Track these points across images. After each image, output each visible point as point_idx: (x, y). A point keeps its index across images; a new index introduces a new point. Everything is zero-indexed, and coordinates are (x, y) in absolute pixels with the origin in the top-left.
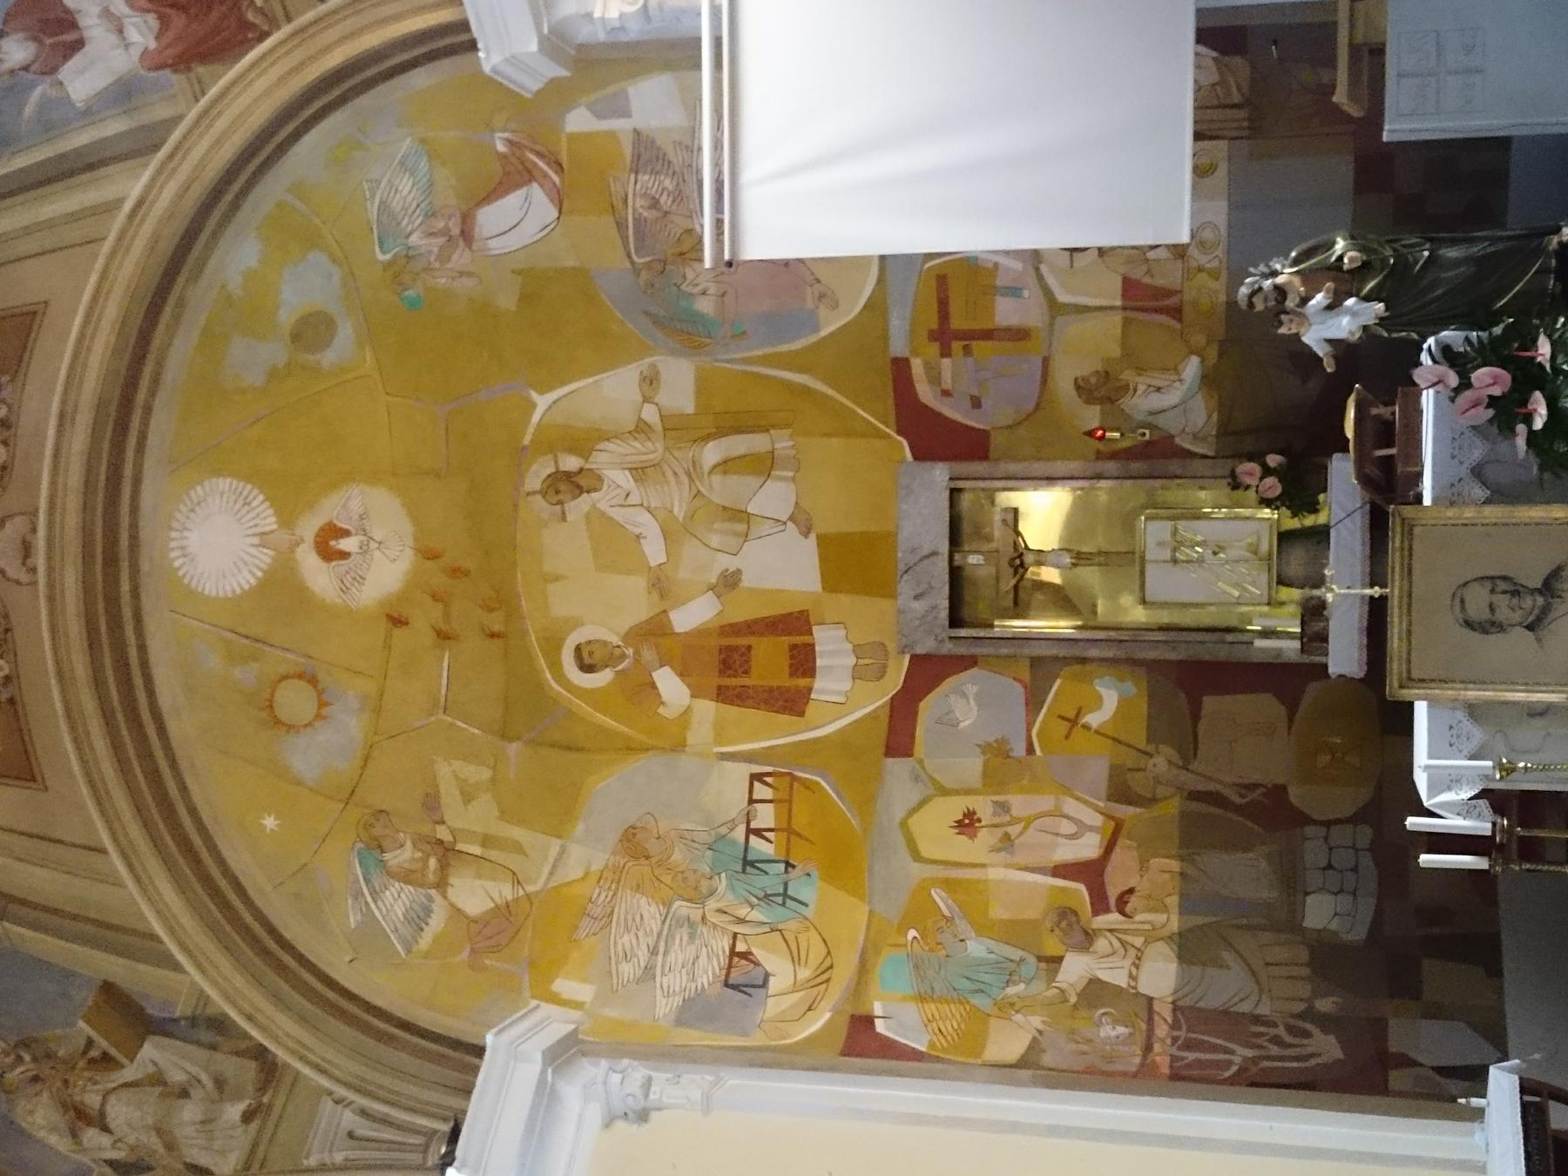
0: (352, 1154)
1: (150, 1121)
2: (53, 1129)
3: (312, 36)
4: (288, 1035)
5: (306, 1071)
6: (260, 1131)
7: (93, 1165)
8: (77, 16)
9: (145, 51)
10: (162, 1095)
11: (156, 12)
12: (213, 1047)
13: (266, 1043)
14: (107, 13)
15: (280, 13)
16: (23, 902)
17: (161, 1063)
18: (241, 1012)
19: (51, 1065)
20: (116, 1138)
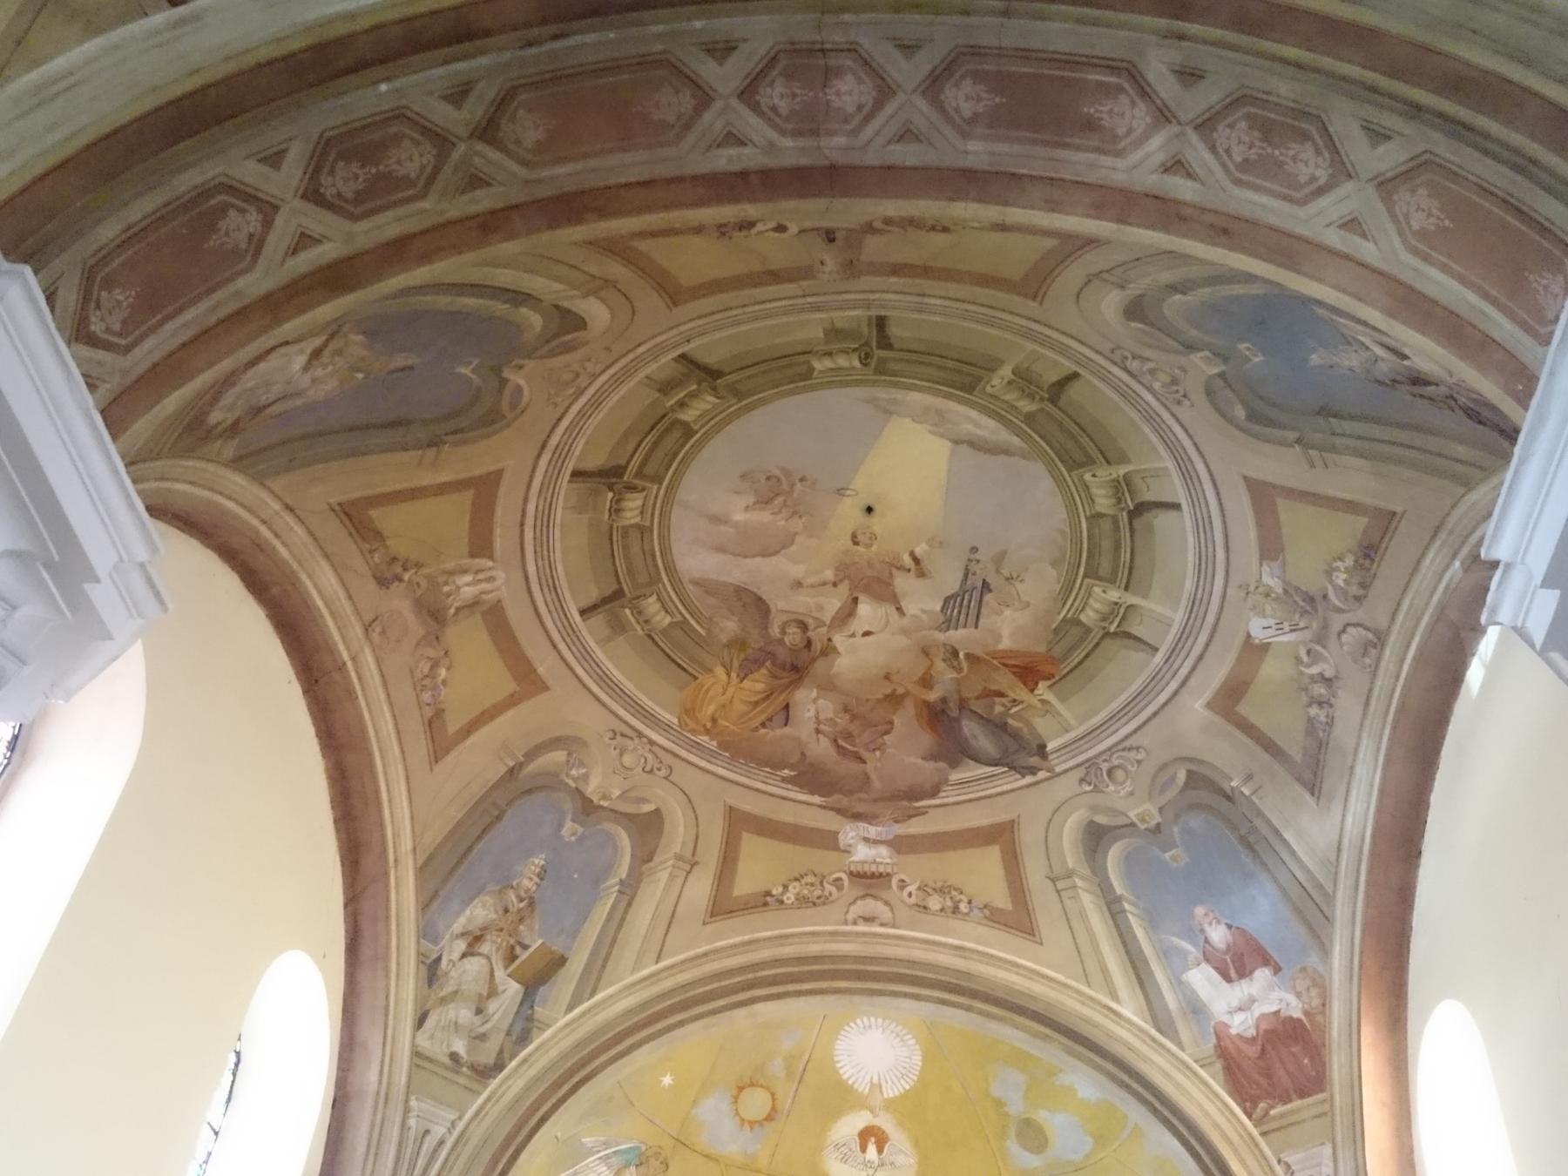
0: (412, 1133)
4: (509, 1087)
5: (480, 1100)
9: (1227, 1026)
10: (480, 995)
12: (508, 1034)
13: (506, 1071)
15: (1266, 1128)
16: (629, 905)
18: (530, 1055)
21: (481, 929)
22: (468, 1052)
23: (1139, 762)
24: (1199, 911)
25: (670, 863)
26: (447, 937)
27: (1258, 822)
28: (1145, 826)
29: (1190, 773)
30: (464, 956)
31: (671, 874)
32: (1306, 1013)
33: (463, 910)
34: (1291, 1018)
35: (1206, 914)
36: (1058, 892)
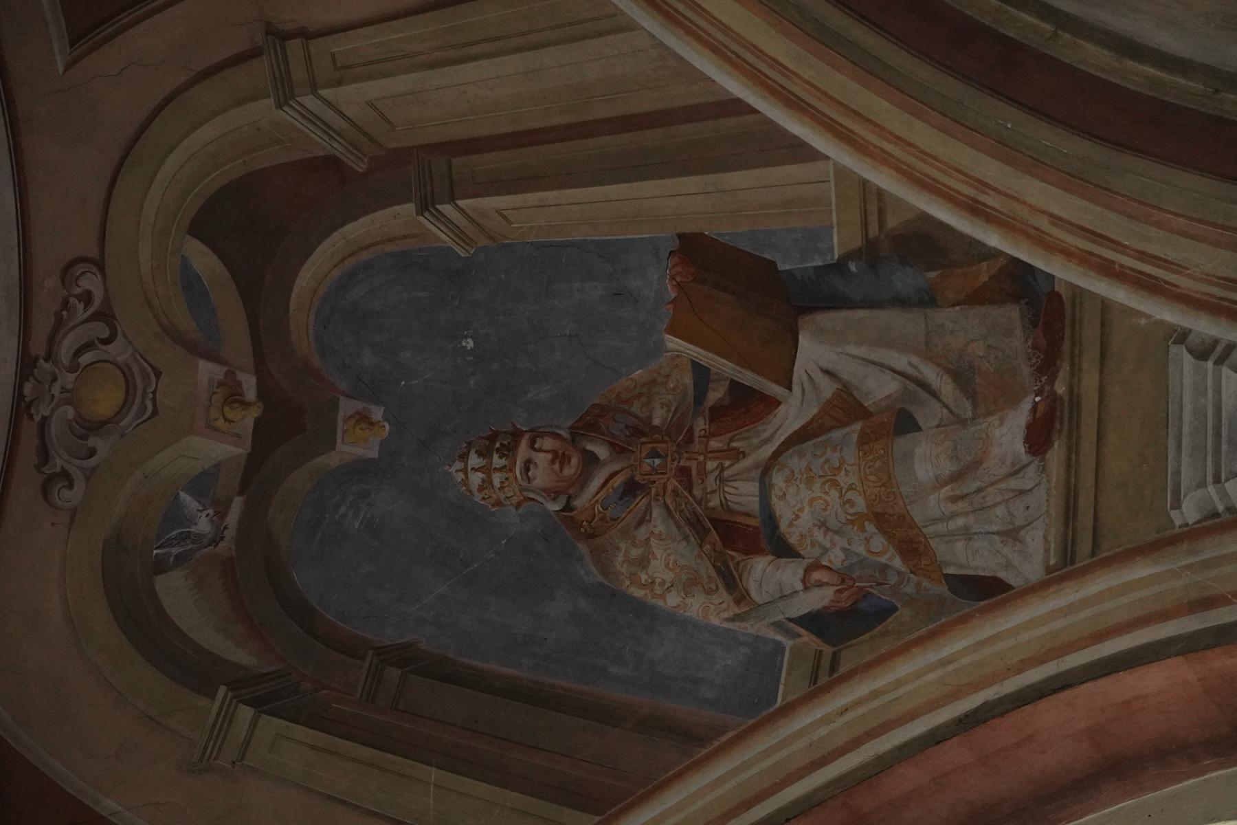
1: (861, 505)
2: (690, 584)
4: (1056, 220)
5: (1120, 295)
6: (1071, 465)
7: (779, 638)
12: (928, 300)
13: (1024, 253)
16: (472, 146)
17: (848, 370)
19: (646, 449)
20: (806, 562)
21: (702, 534)
22: (1015, 401)
25: (308, 101)
26: (751, 628)
30: (784, 550)
31: (340, 83)
33: (672, 619)
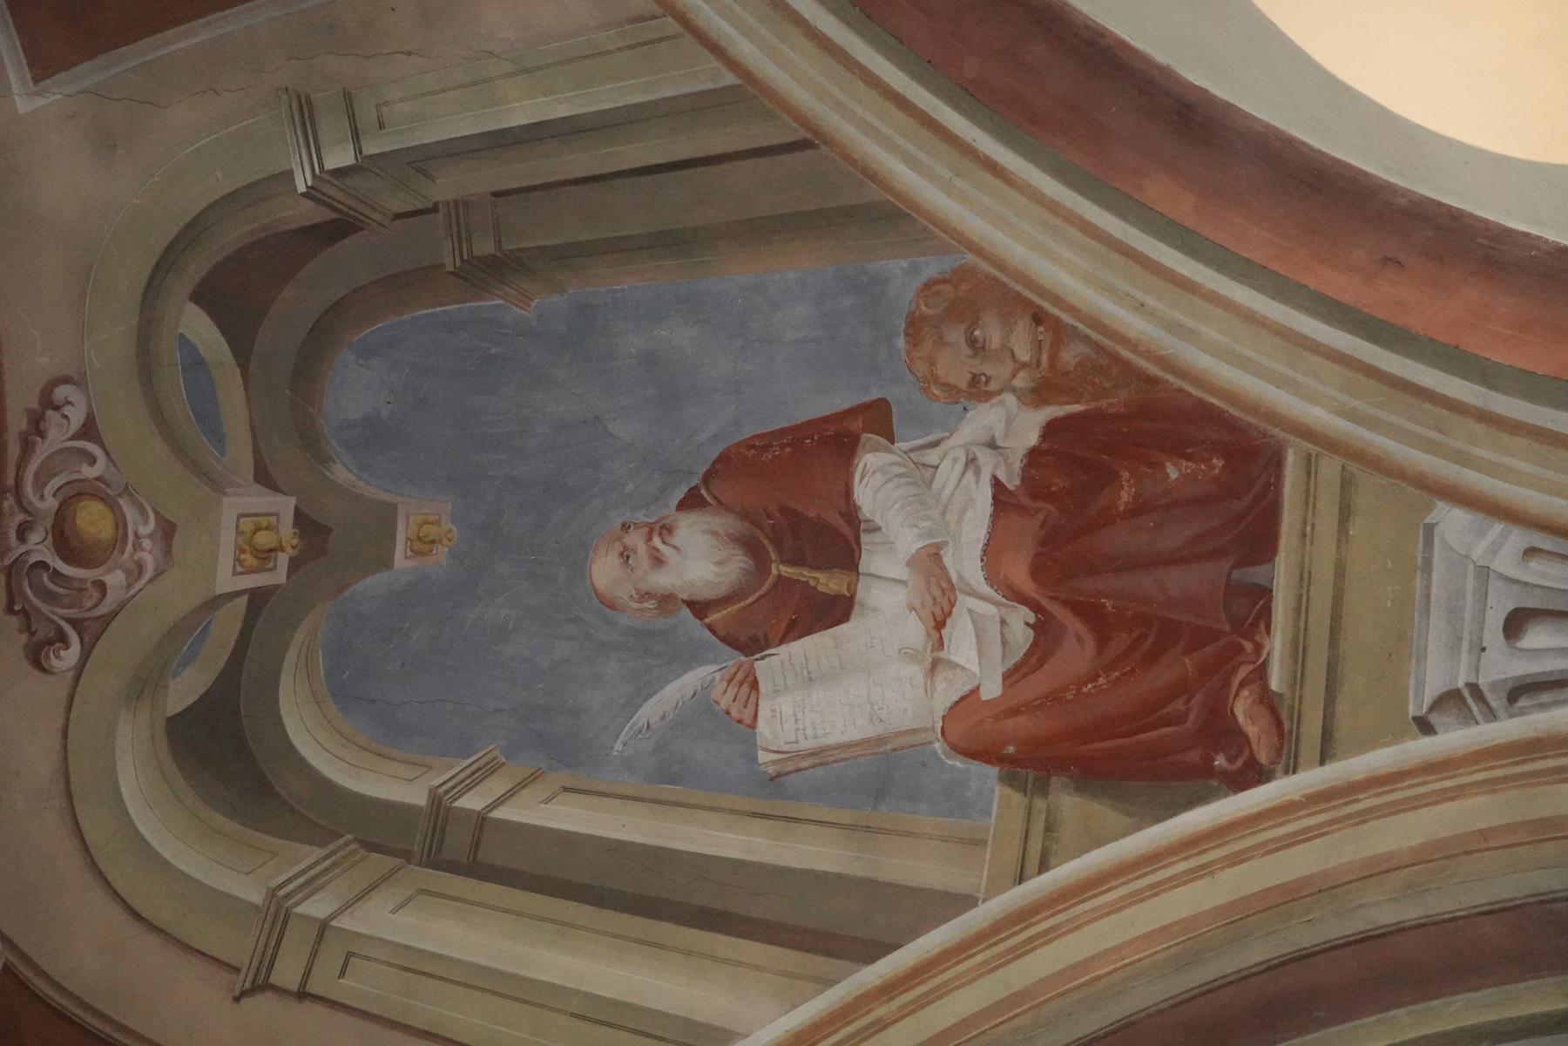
3: (1363, 817)
8: (865, 538)
11: (1036, 607)
14: (931, 561)
15: (1312, 728)
23: (89, 430)
24: (605, 571)
27: (446, 186)
28: (283, 560)
29: (205, 296)
32: (1039, 394)
34: (1033, 457)
35: (625, 555)
36: (302, 995)
